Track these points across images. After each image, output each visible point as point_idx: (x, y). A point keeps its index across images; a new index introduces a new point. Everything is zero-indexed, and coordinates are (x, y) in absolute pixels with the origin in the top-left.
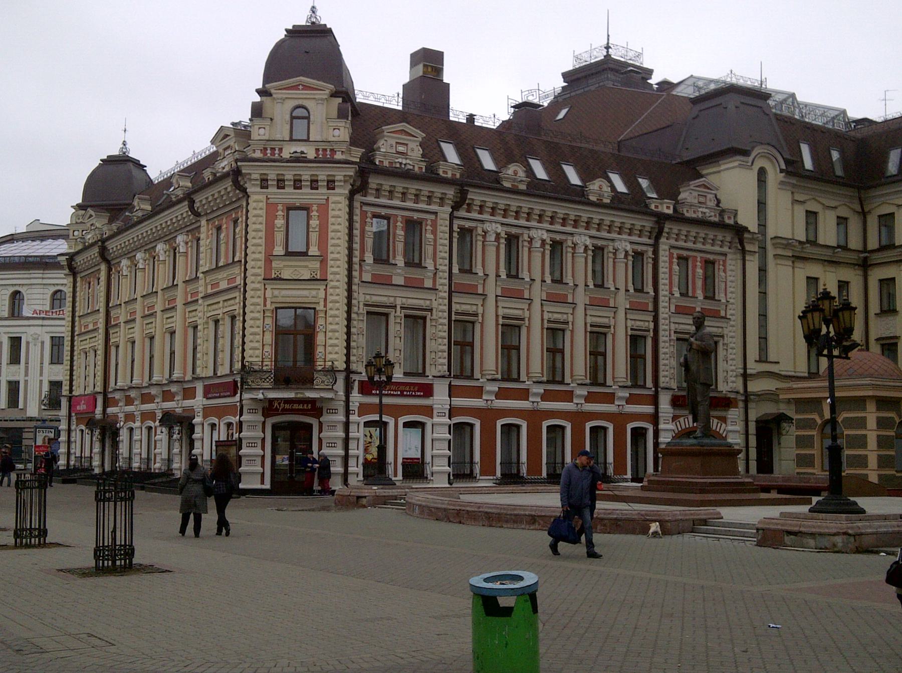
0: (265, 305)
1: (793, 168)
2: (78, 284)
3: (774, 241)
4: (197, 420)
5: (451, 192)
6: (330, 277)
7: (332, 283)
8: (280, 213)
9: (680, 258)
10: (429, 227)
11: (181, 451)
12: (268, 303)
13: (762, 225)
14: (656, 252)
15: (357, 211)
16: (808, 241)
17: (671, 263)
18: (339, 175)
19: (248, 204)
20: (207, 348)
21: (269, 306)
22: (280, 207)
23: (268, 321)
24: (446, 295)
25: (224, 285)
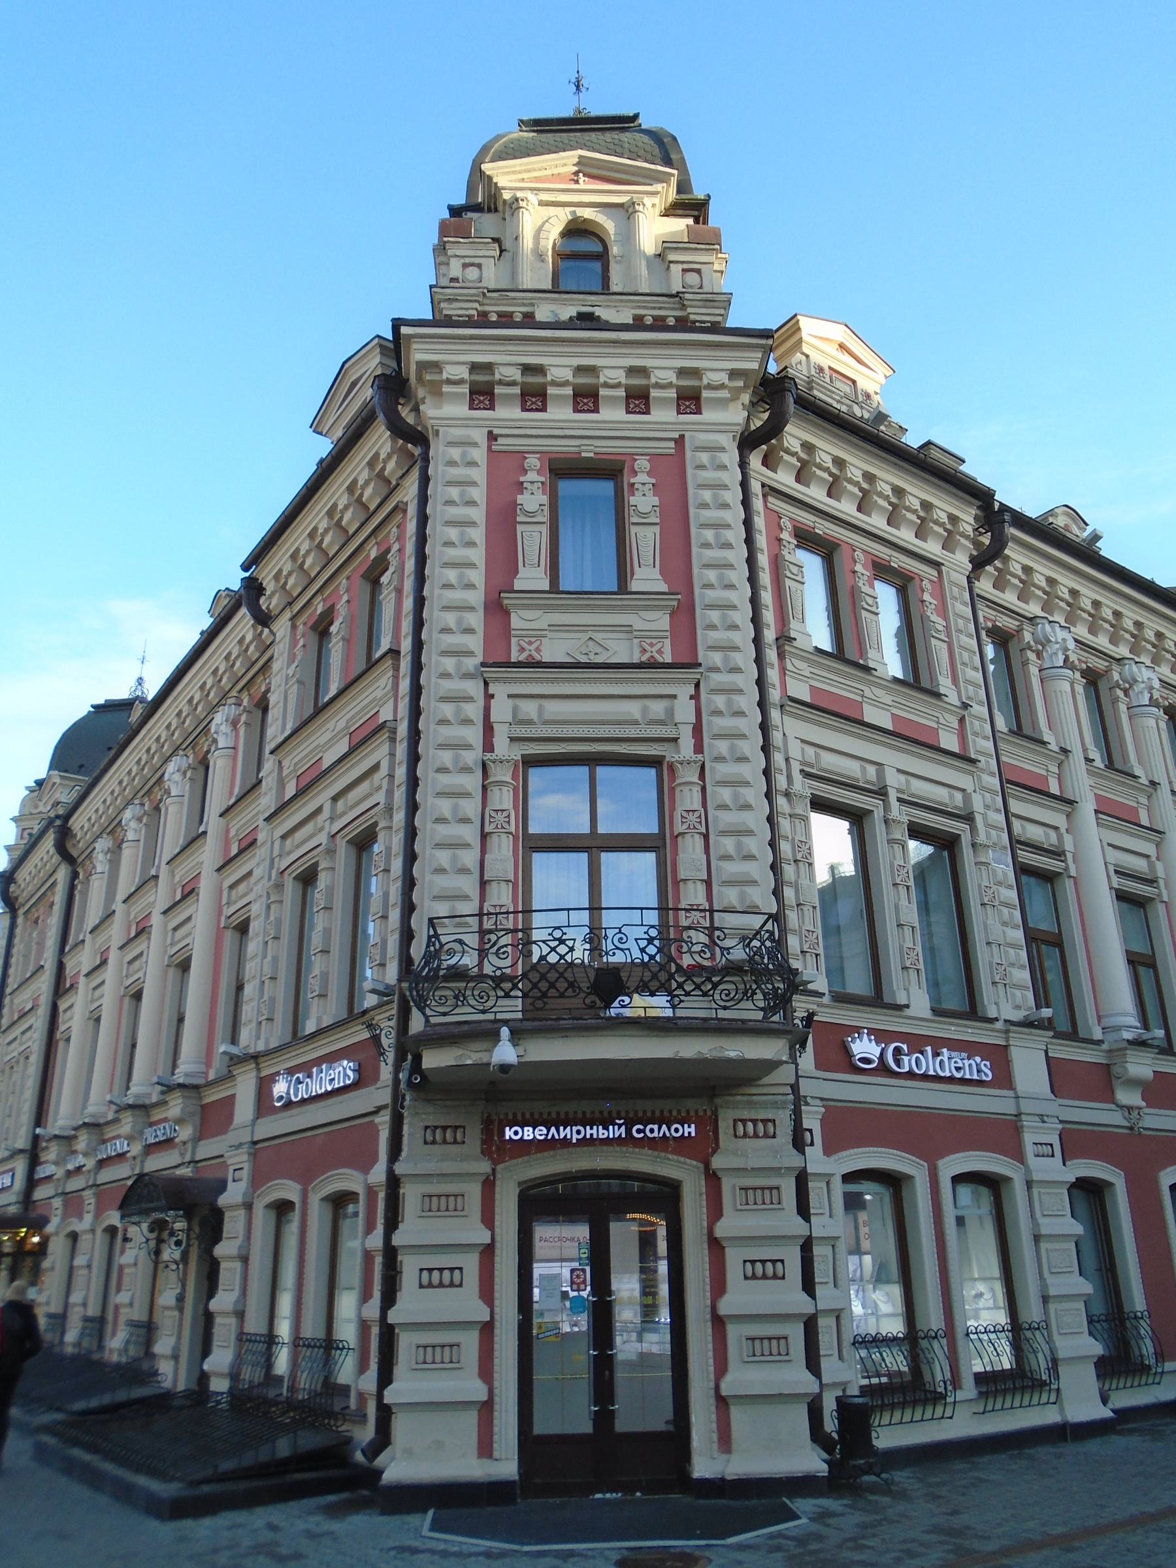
0: (488, 746)
2: (18, 931)
4: (233, 1195)
7: (716, 677)
8: (532, 476)
11: (181, 1299)
15: (758, 504)
20: (275, 960)
22: (533, 461)
23: (503, 799)
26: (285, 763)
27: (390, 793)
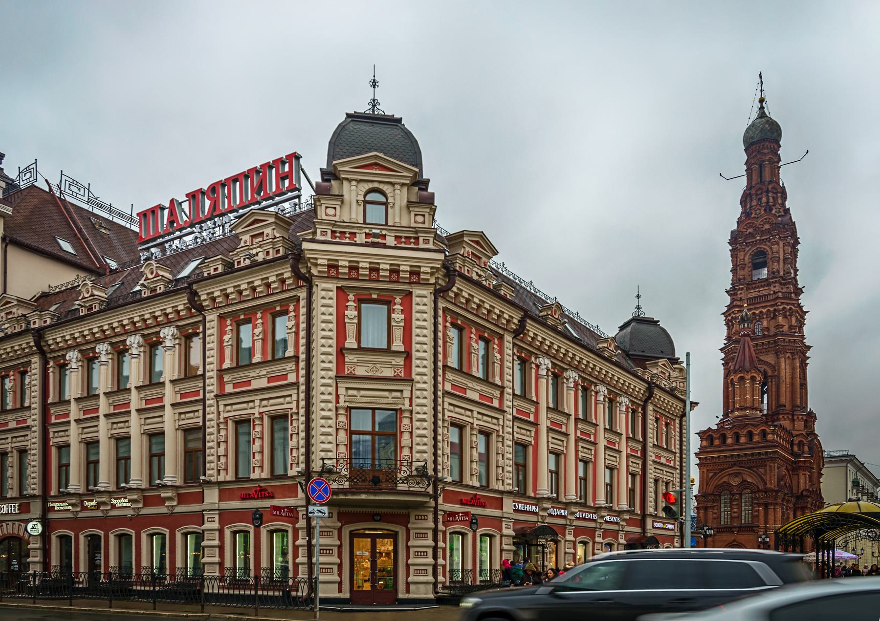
0: (337, 402)
12: (342, 399)
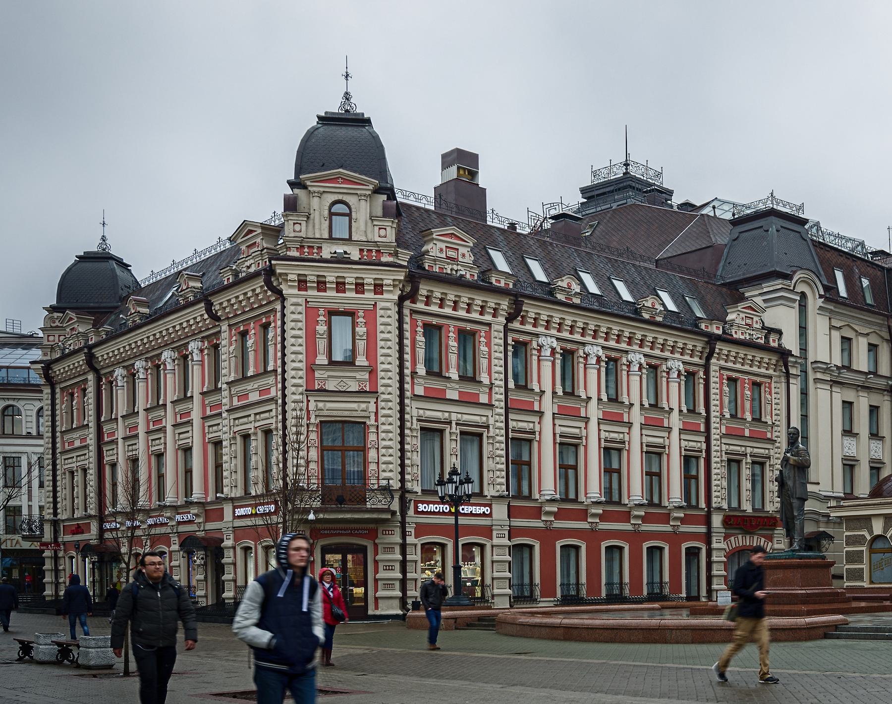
1: (830, 290)
3: (814, 366)
5: (505, 304)
6: (381, 389)
9: (729, 379)
10: (482, 339)
13: (804, 350)
14: (707, 373)
15: (407, 319)
16: (844, 367)
17: (722, 384)
18: (388, 278)
19: (283, 307)
21: (313, 420)
24: (503, 411)
25: (254, 397)
26: (233, 389)
27: (276, 422)
